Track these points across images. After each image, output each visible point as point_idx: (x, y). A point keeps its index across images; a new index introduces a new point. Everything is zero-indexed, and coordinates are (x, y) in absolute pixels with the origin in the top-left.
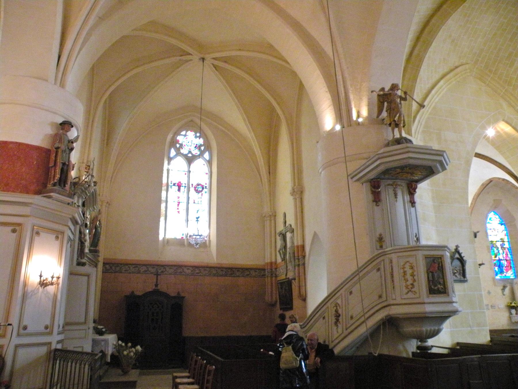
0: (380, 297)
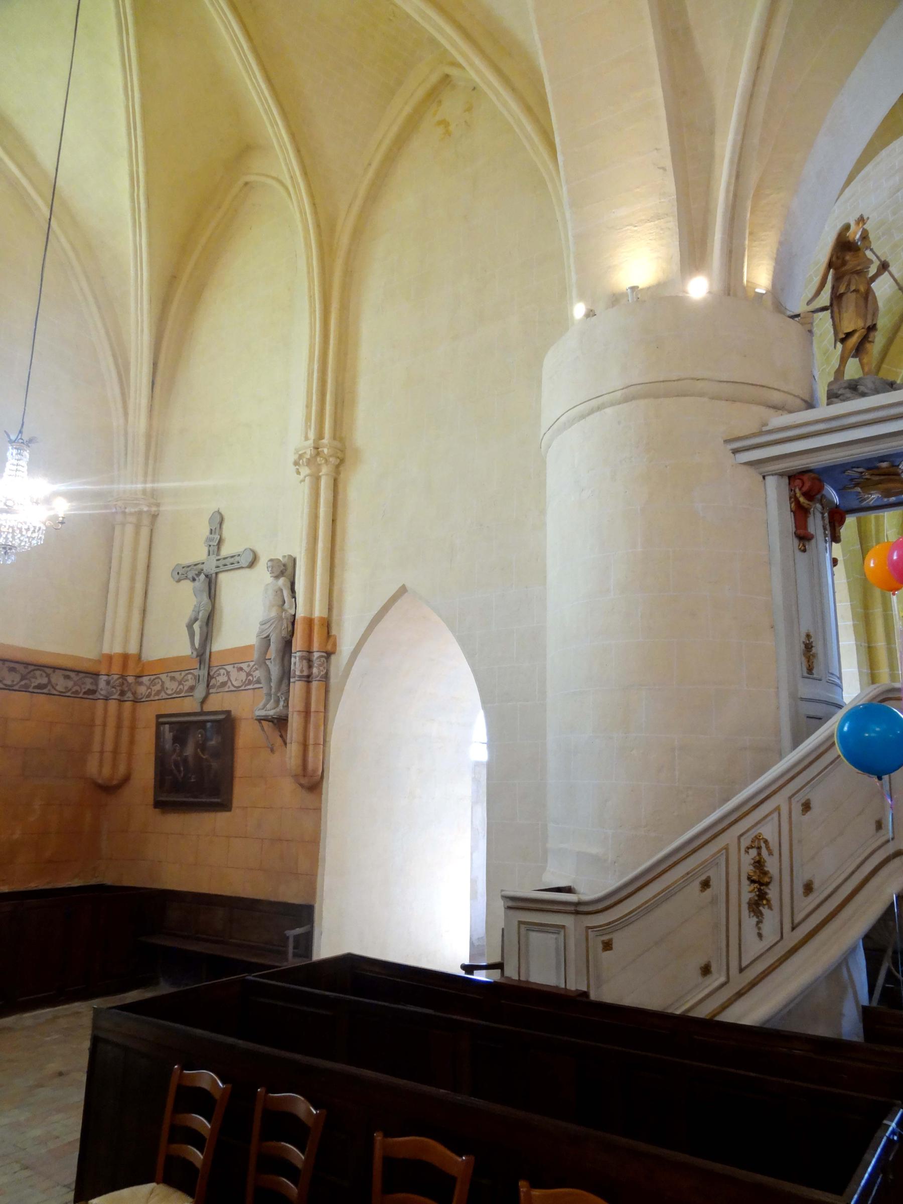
0: (879, 825)
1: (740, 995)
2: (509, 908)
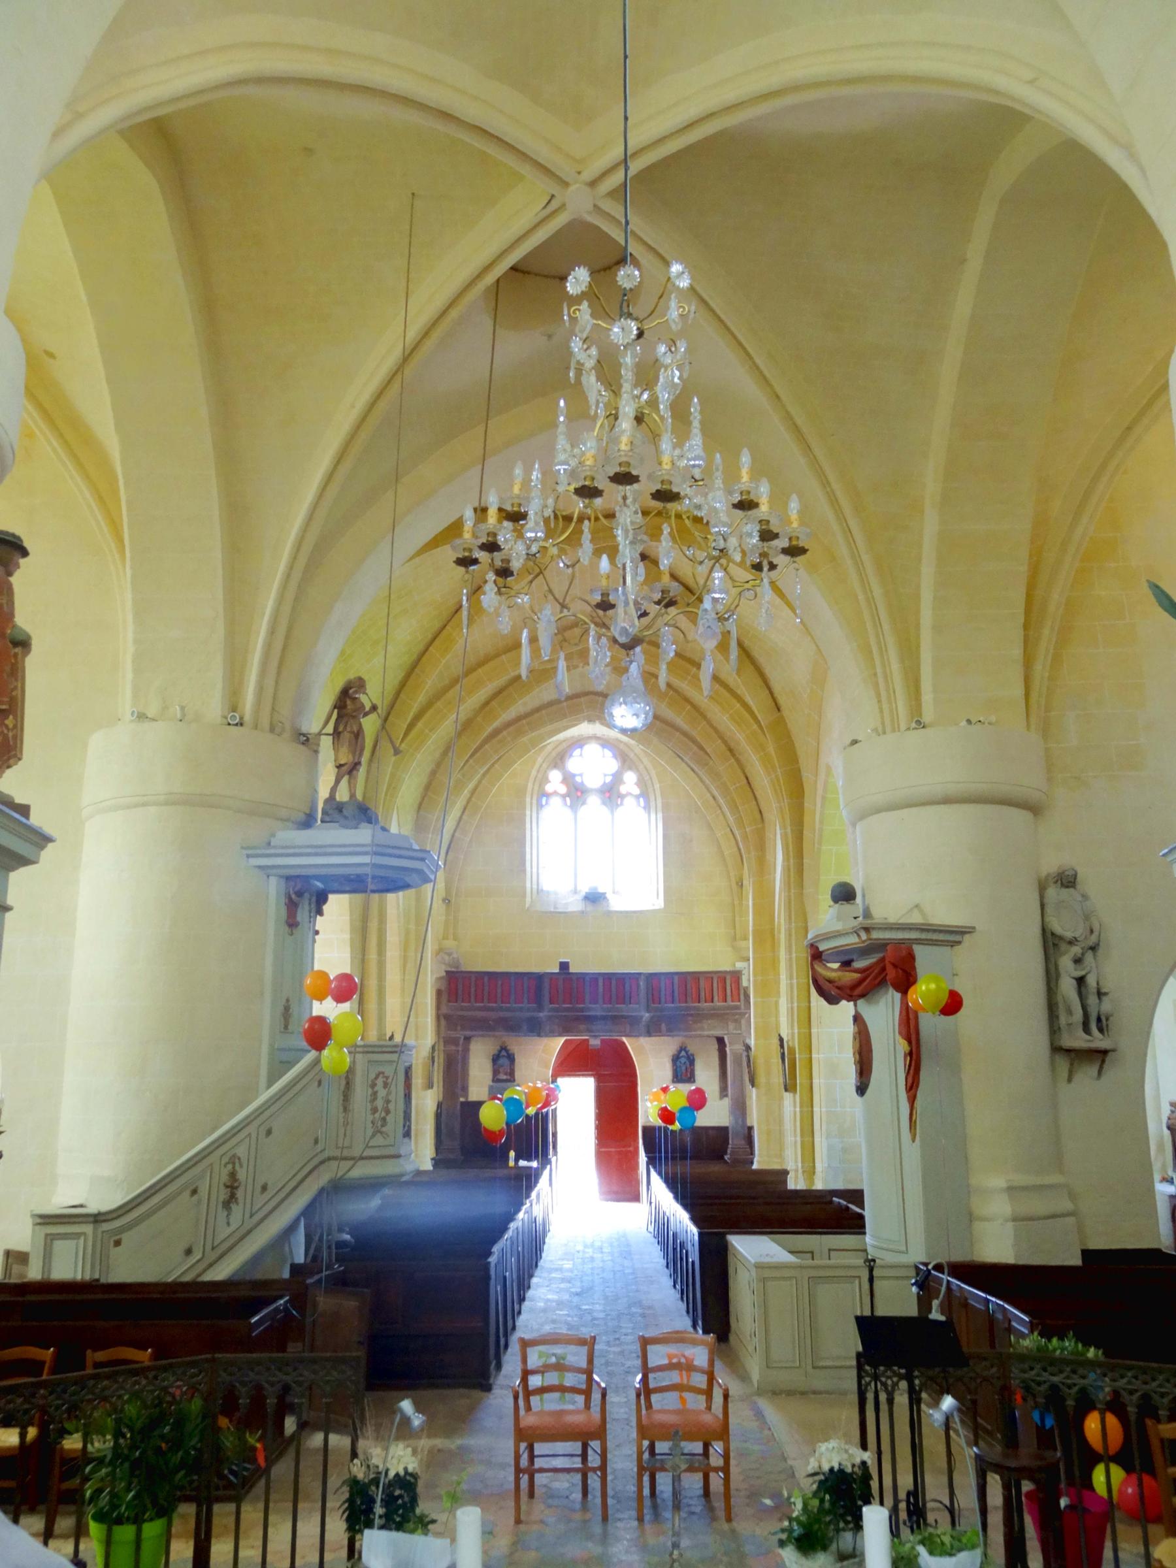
0: (316, 1142)
1: (211, 1265)
2: (39, 1224)
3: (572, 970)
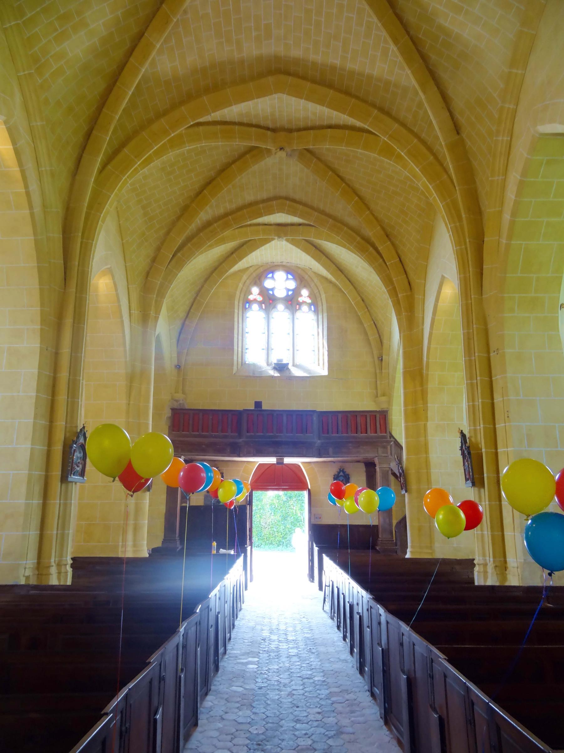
3: (264, 407)
